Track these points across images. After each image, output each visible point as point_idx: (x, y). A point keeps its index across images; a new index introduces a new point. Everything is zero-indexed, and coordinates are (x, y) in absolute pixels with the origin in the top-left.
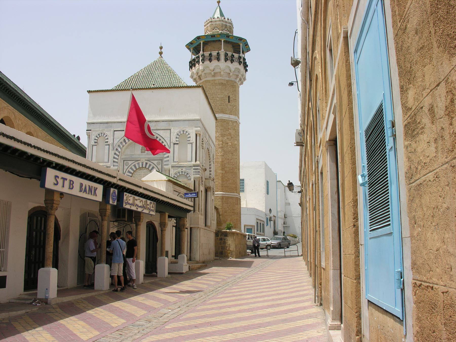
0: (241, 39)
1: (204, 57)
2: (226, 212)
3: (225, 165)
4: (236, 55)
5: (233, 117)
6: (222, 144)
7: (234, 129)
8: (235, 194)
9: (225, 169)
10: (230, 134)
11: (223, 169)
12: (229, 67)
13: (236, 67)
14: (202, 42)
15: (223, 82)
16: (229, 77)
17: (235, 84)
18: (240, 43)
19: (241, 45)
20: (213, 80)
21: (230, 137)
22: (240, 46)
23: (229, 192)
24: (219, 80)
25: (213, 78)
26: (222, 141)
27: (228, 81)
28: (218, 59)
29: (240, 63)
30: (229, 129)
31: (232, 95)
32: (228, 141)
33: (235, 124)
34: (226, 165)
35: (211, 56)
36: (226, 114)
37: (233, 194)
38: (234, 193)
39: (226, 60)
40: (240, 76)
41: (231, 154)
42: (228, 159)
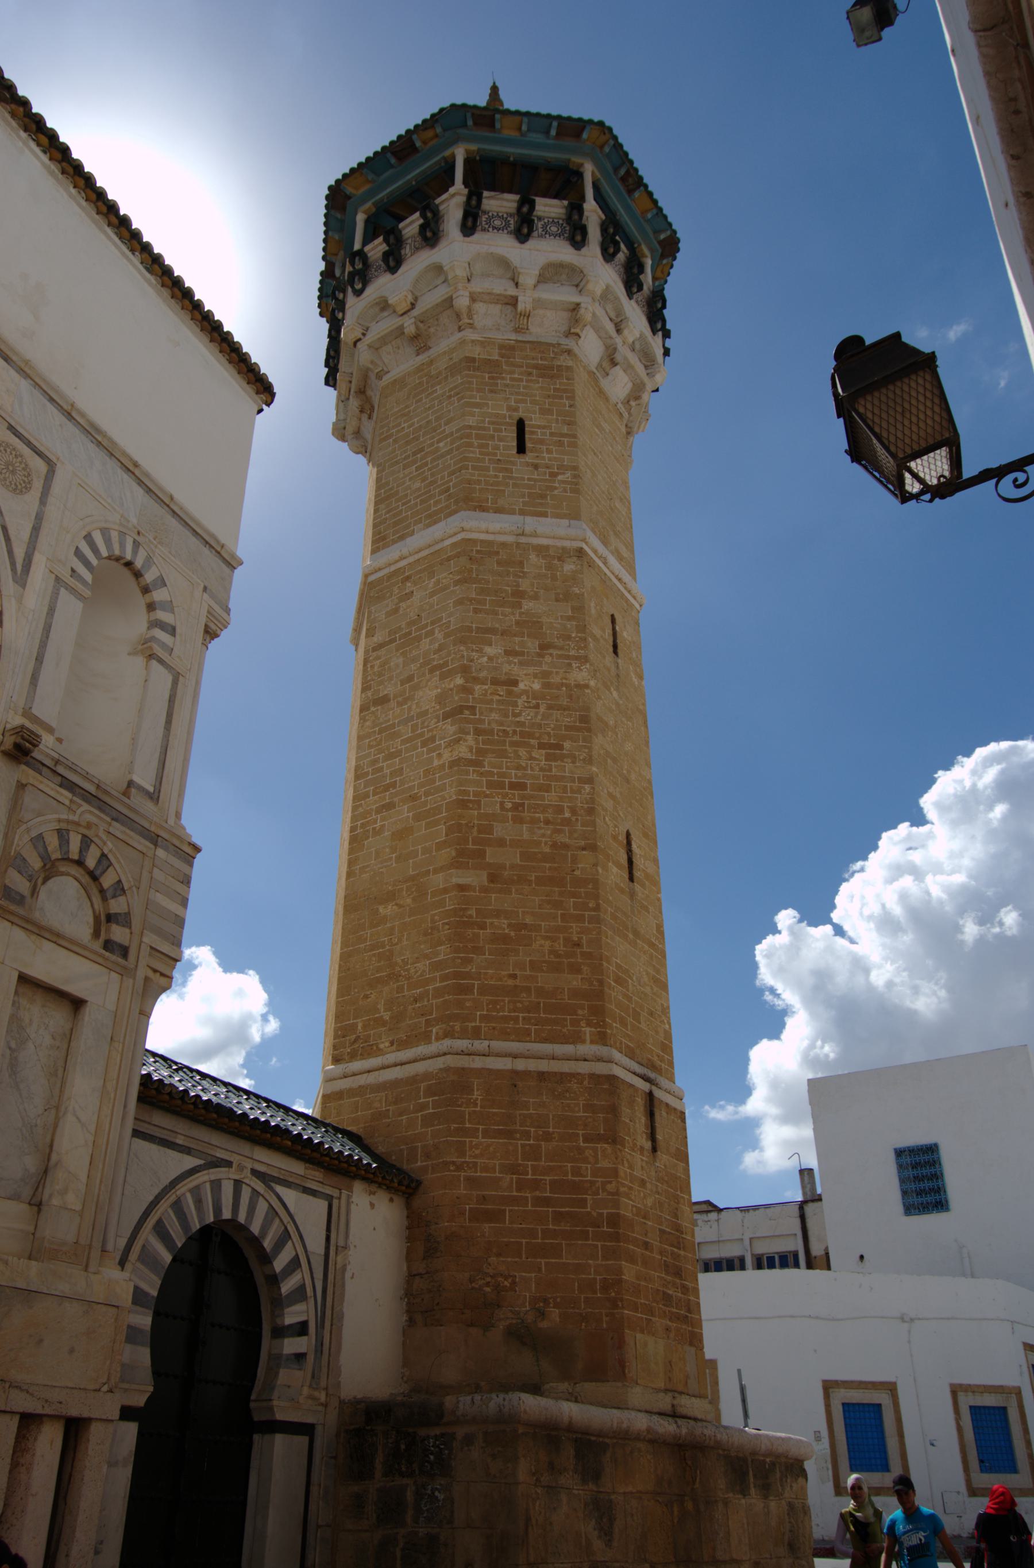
0: (572, 128)
2: (494, 1216)
3: (489, 829)
4: (549, 208)
5: (550, 530)
6: (465, 690)
7: (566, 597)
8: (586, 1049)
9: (492, 856)
10: (531, 625)
11: (467, 855)
12: (504, 263)
14: (360, 218)
15: (477, 352)
16: (517, 330)
17: (564, 361)
18: (576, 159)
19: (589, 170)
20: (419, 369)
21: (532, 646)
22: (580, 175)
23: (522, 1036)
25: (423, 358)
26: (465, 670)
27: (508, 350)
28: (431, 235)
29: (577, 235)
30: (519, 594)
31: (544, 412)
32: (511, 668)
33: (569, 567)
34: (499, 830)
36: (499, 511)
37: (569, 1049)
38: (576, 1038)
40: (590, 309)
41: (539, 754)
42: (513, 786)
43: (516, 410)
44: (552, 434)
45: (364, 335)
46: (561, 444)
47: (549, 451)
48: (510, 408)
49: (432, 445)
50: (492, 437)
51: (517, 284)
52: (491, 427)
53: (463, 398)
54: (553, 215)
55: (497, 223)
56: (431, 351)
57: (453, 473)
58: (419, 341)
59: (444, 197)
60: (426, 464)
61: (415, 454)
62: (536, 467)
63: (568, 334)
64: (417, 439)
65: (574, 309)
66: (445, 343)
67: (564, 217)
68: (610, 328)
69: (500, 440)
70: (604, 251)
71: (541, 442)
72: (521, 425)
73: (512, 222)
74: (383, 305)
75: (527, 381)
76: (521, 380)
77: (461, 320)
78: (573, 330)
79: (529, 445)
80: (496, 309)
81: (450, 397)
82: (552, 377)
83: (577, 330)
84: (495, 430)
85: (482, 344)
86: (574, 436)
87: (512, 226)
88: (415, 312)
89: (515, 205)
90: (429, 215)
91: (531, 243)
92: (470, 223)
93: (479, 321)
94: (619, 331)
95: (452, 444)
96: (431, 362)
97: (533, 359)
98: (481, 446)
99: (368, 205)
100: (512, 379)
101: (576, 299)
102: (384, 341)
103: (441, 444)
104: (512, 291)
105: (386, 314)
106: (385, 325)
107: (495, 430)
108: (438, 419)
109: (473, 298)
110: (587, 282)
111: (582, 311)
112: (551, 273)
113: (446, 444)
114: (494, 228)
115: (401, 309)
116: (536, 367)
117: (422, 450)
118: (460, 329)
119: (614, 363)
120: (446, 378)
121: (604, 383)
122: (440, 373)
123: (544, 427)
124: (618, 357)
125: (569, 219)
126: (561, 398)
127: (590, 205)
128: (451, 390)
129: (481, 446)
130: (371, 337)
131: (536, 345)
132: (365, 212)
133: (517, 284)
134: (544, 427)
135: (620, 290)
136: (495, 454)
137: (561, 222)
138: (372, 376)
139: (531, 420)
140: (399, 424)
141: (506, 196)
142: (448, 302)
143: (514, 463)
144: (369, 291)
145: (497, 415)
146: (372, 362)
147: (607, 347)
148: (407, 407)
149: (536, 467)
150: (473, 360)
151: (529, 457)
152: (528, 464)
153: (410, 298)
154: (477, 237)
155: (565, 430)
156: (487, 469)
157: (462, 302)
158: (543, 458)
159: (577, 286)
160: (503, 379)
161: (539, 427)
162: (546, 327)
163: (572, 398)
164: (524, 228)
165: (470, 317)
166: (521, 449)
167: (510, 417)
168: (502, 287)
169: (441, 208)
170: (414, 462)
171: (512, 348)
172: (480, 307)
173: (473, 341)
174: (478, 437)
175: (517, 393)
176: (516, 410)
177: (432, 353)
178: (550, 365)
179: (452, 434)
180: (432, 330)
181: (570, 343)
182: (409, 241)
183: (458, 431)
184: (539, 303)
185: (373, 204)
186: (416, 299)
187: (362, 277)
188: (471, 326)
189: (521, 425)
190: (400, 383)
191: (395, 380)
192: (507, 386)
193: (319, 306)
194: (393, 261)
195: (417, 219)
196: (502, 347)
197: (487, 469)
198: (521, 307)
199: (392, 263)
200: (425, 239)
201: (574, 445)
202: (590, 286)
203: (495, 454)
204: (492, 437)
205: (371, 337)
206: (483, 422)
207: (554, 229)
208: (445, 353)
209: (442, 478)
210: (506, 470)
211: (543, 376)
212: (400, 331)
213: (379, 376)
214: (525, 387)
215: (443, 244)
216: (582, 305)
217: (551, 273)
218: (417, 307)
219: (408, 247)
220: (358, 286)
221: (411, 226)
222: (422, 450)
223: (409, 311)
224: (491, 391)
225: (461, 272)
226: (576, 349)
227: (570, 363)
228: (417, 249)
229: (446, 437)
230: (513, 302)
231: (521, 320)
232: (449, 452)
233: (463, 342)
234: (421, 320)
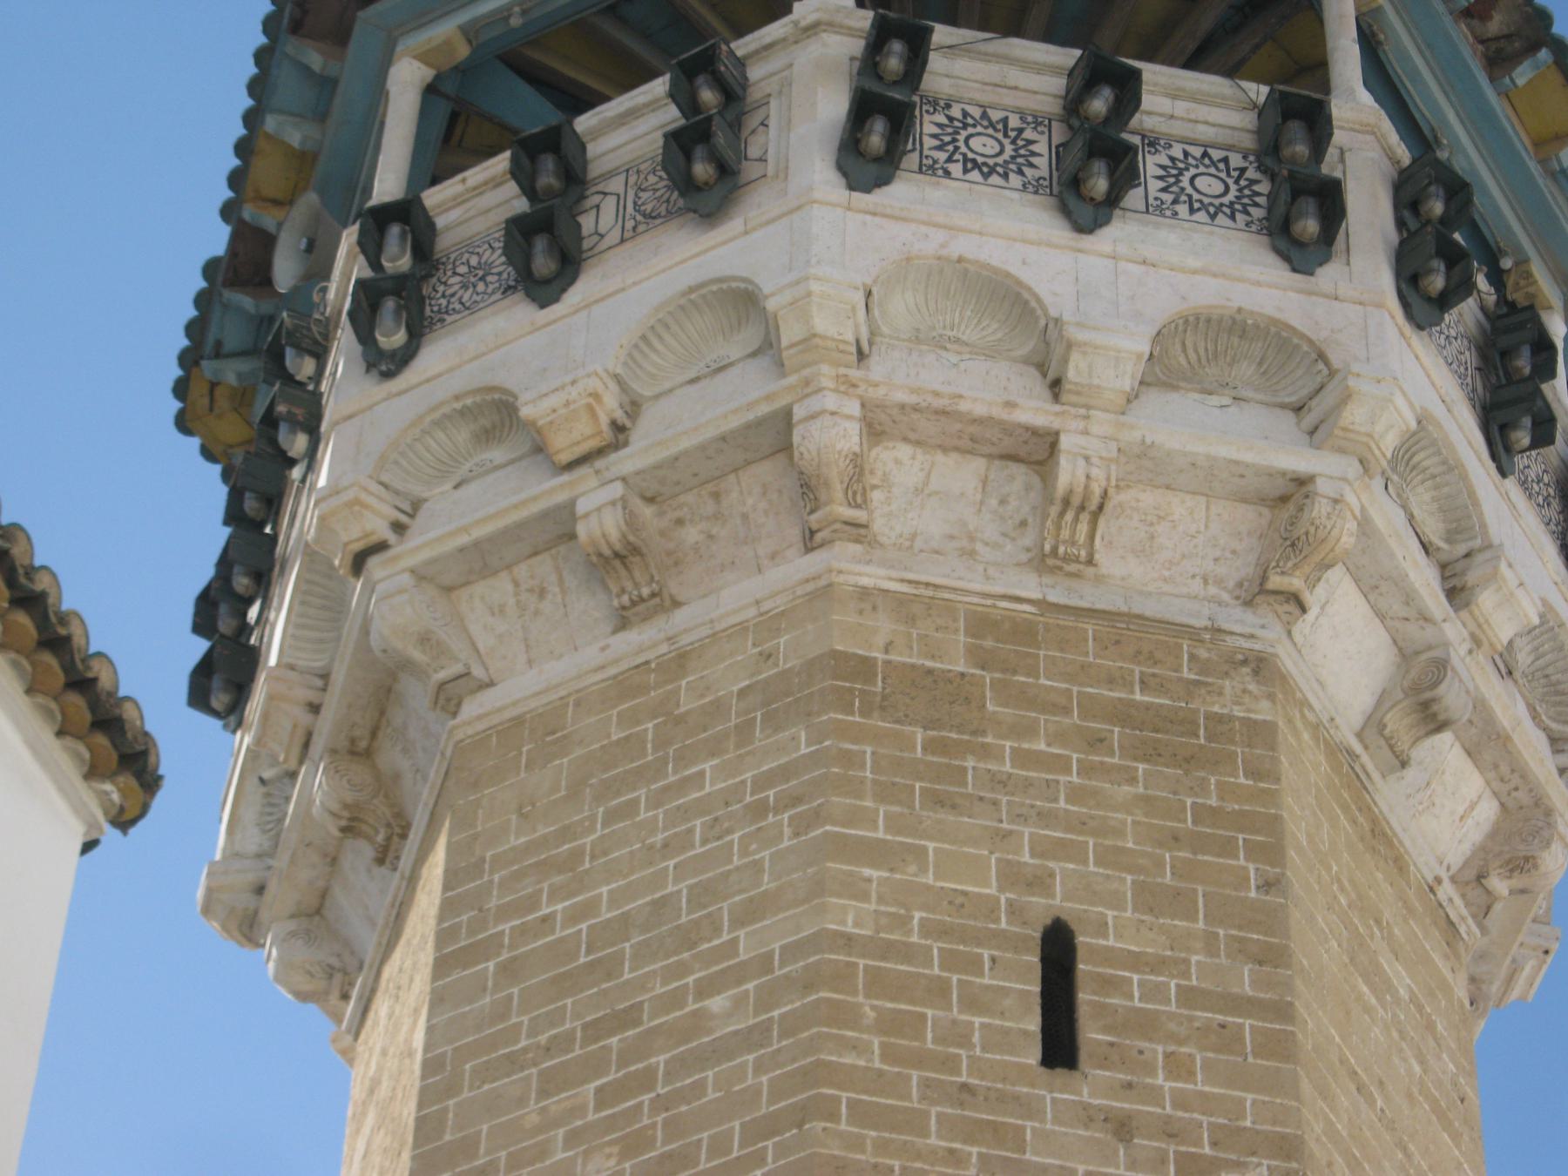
1: (423, 250)
4: (1193, 108)
12: (1010, 301)
13: (1207, 294)
14: (406, 79)
15: (877, 639)
16: (1046, 561)
17: (1235, 698)
20: (625, 686)
24: (770, 624)
25: (644, 640)
27: (1005, 636)
28: (706, 168)
31: (1151, 899)
35: (575, 178)
39: (882, 128)
40: (1357, 503)
43: (1039, 882)
44: (1189, 996)
45: (399, 528)
46: (1227, 1039)
47: (1178, 1067)
48: (1011, 875)
49: (675, 1000)
50: (939, 991)
51: (1056, 386)
52: (936, 947)
53: (817, 817)
54: (1204, 133)
55: (983, 146)
56: (680, 617)
57: (769, 1127)
58: (628, 574)
59: (774, 31)
60: (646, 1080)
61: (594, 1031)
62: (1123, 1128)
63: (1257, 592)
64: (609, 967)
65: (1284, 499)
66: (738, 590)
67: (1248, 142)
68: (1424, 579)
69: (972, 1002)
70: (1409, 279)
71: (1146, 1024)
72: (1058, 951)
73: (1041, 147)
74: (495, 416)
75: (1086, 770)
76: (1063, 765)
77: (817, 510)
78: (1276, 581)
79: (1091, 1034)
80: (962, 475)
81: (760, 810)
82: (1189, 761)
83: (1296, 583)
84: (951, 961)
85: (904, 606)
86: (1284, 1011)
87: (1042, 162)
88: (627, 461)
89: (1058, 84)
90: (708, 96)
91: (1119, 233)
92: (876, 139)
93: (888, 515)
94: (1456, 593)
95: (766, 999)
96: (680, 661)
97: (1111, 681)
98: (890, 1024)
99: (445, 30)
100: (1021, 758)
101: (1298, 460)
102: (481, 559)
103: (717, 1003)
104: (1035, 411)
105: (497, 454)
106: (504, 495)
107: (951, 961)
108: (703, 894)
109: (877, 426)
110: (1346, 397)
111: (1320, 509)
112: (1197, 352)
113: (739, 1002)
114: (970, 164)
115: (565, 444)
116: (1123, 714)
117: (629, 1017)
118: (811, 541)
119: (1432, 720)
120: (744, 731)
121: (1391, 795)
122: (718, 708)
123: (1157, 965)
124: (1452, 698)
125: (1269, 150)
126: (1227, 848)
127: (1353, 104)
128: (761, 783)
129: (890, 1024)
130: (434, 536)
131: (1125, 629)
132: (423, 58)
133: (1056, 386)
134: (1157, 965)
135: (1463, 433)
136: (950, 1063)
137: (1236, 160)
138: (417, 696)
139: (1101, 928)
140: (532, 903)
141: (1020, 47)
142: (775, 435)
143: (1029, 1108)
144: (434, 357)
145: (960, 901)
146: (424, 639)
147: (1405, 655)
148: (565, 834)
149: (1123, 1128)
150: (864, 668)
151: (1090, 1086)
152: (1088, 1116)
153: (611, 404)
154: (903, 191)
155: (1245, 981)
156: (915, 1122)
157: (831, 434)
158: (1155, 1095)
159: (1298, 409)
160: (985, 752)
161: (1136, 961)
162: (1167, 559)
163: (1271, 852)
164: (1093, 169)
165: (857, 494)
166: (1060, 1049)
167: (1014, 910)
168: (997, 389)
169: (755, 73)
170: (595, 1065)
171: (1023, 632)
172: (899, 464)
173: (864, 593)
174: (877, 983)
175: (1045, 818)
176: (1039, 882)
177: (689, 622)
178: (1186, 715)
179: (764, 963)
180: (691, 534)
181: (1256, 628)
182: (616, 185)
183: (790, 953)
184: (1146, 464)
185: (467, 31)
186: (634, 407)
187: (403, 306)
188: (858, 531)
189: (1058, 951)
190: (538, 731)
191: (518, 721)
192: (1001, 782)
193: (181, 389)
194: (545, 253)
195: (652, 106)
196: (981, 624)
197: (915, 1122)
198: (1068, 473)
199: (543, 264)
200: (686, 185)
201: (1280, 1047)
202: (1355, 416)
203: (950, 1063)
204: (939, 991)
205: (434, 536)
206: (903, 922)
207: (1209, 185)
208: (742, 628)
209: (719, 1146)
210: (997, 1133)
211: (1152, 754)
212: (558, 528)
213: (448, 698)
214: (1075, 795)
215: (758, 205)
216: (1322, 486)
217: (1197, 352)
218: (639, 437)
219: (609, 205)
220: (392, 338)
221: (628, 129)
222: (629, 1017)
223: (600, 452)
224: (938, 801)
225: (834, 322)
226: (1287, 659)
227: (1263, 711)
228: (649, 216)
229: (739, 974)
230: (1037, 452)
231: (1065, 521)
232: (755, 1037)
233: (822, 594)
234: (652, 491)
